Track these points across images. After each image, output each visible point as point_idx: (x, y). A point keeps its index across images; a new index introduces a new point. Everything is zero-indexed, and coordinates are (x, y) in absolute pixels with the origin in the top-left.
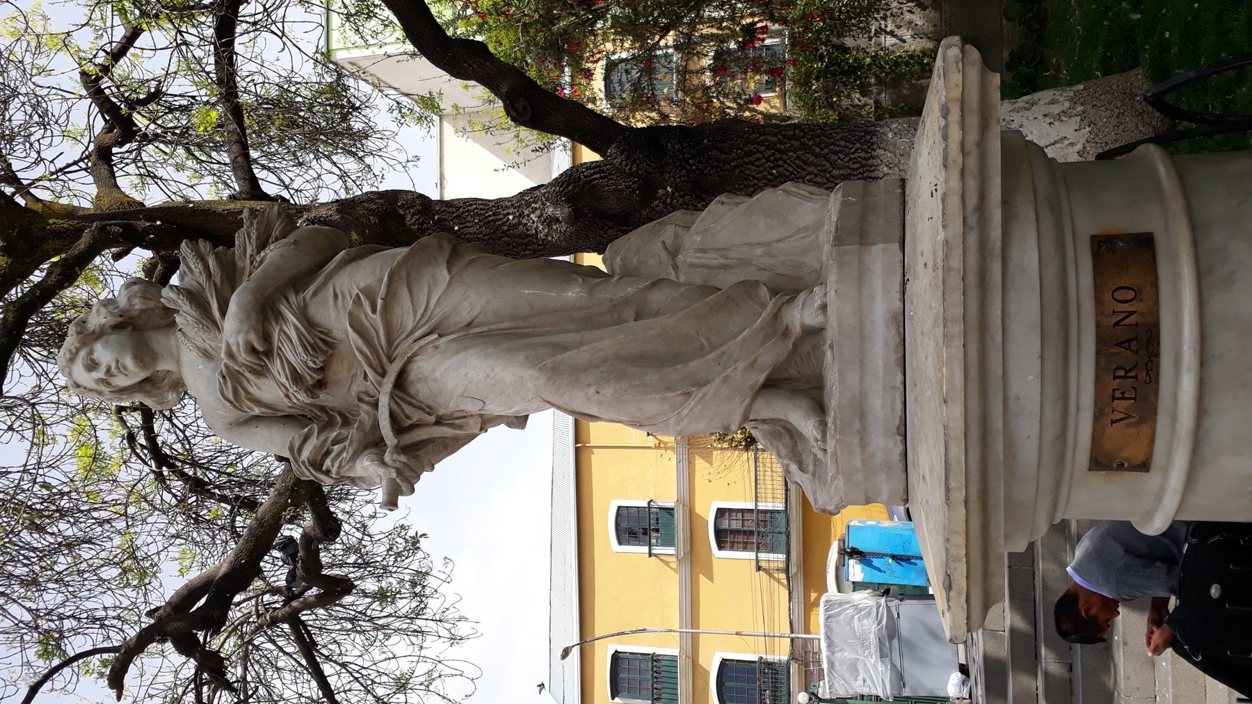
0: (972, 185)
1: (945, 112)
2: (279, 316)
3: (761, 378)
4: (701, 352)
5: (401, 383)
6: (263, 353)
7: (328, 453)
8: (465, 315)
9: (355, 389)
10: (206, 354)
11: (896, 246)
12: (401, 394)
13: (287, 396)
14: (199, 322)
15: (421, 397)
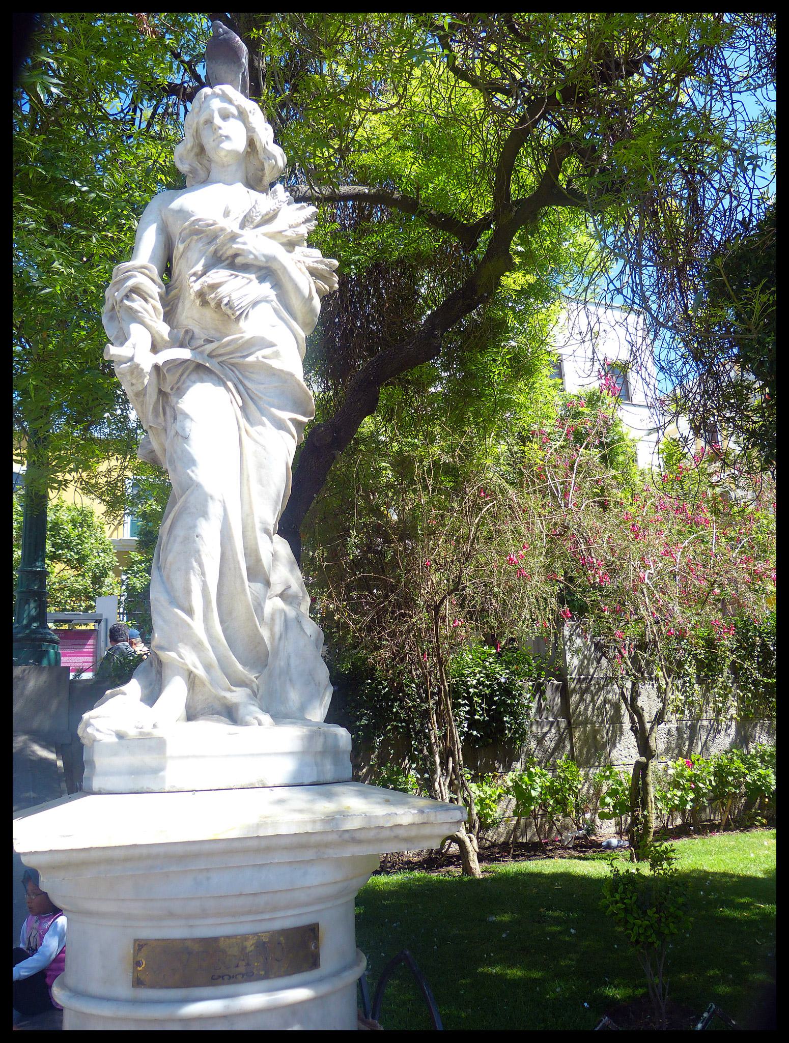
0: (372, 834)
11: (314, 779)
12: (191, 368)
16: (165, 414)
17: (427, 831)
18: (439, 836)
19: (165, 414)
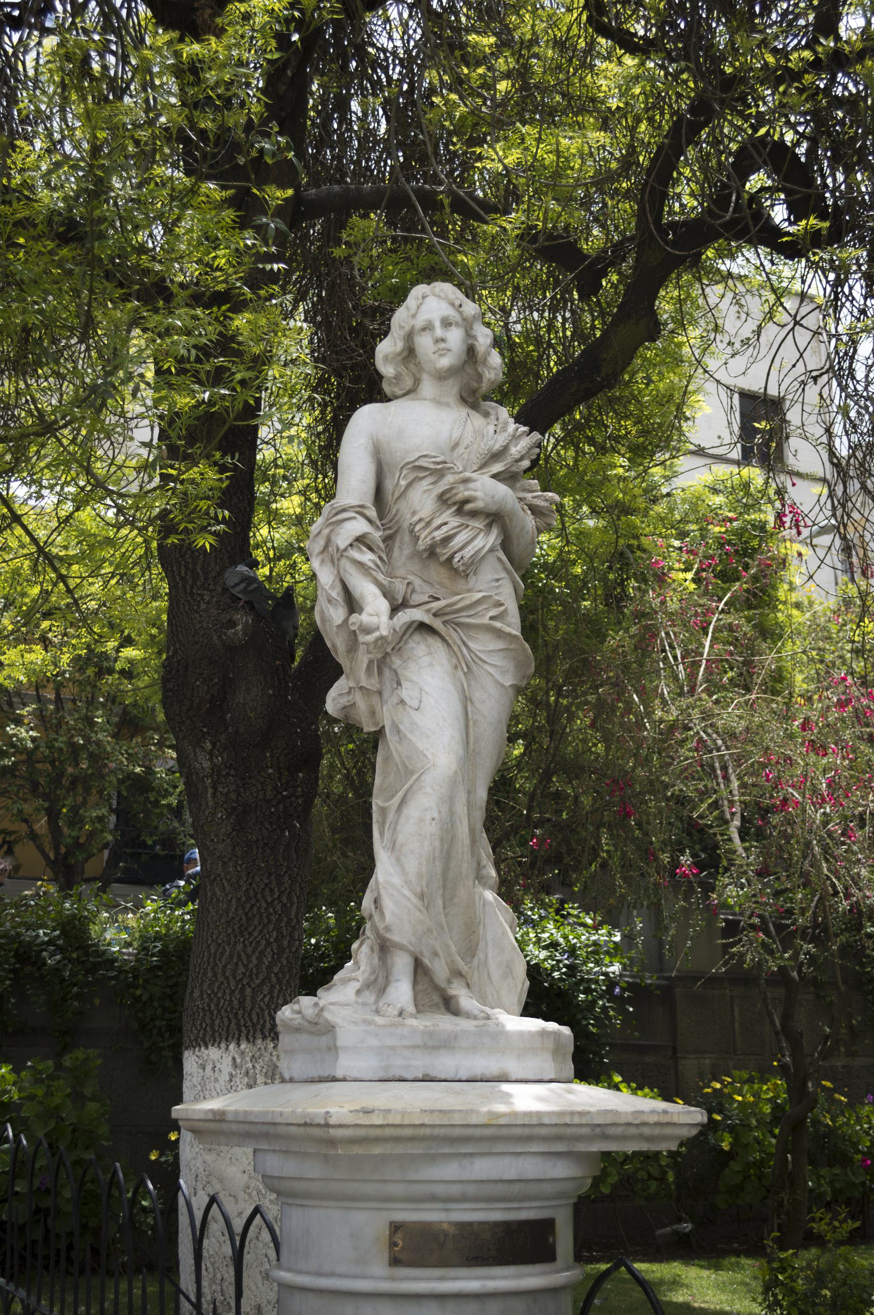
0: (619, 1131)
1: (665, 1112)
2: (489, 526)
3: (426, 961)
4: (444, 908)
5: (423, 627)
6: (463, 508)
7: (371, 549)
8: (477, 695)
9: (417, 582)
10: (456, 445)
11: (552, 1076)
13: (421, 520)
14: (489, 450)
15: (411, 644)
16: (380, 673)
17: (669, 1131)
18: (677, 1137)
19: (380, 673)
